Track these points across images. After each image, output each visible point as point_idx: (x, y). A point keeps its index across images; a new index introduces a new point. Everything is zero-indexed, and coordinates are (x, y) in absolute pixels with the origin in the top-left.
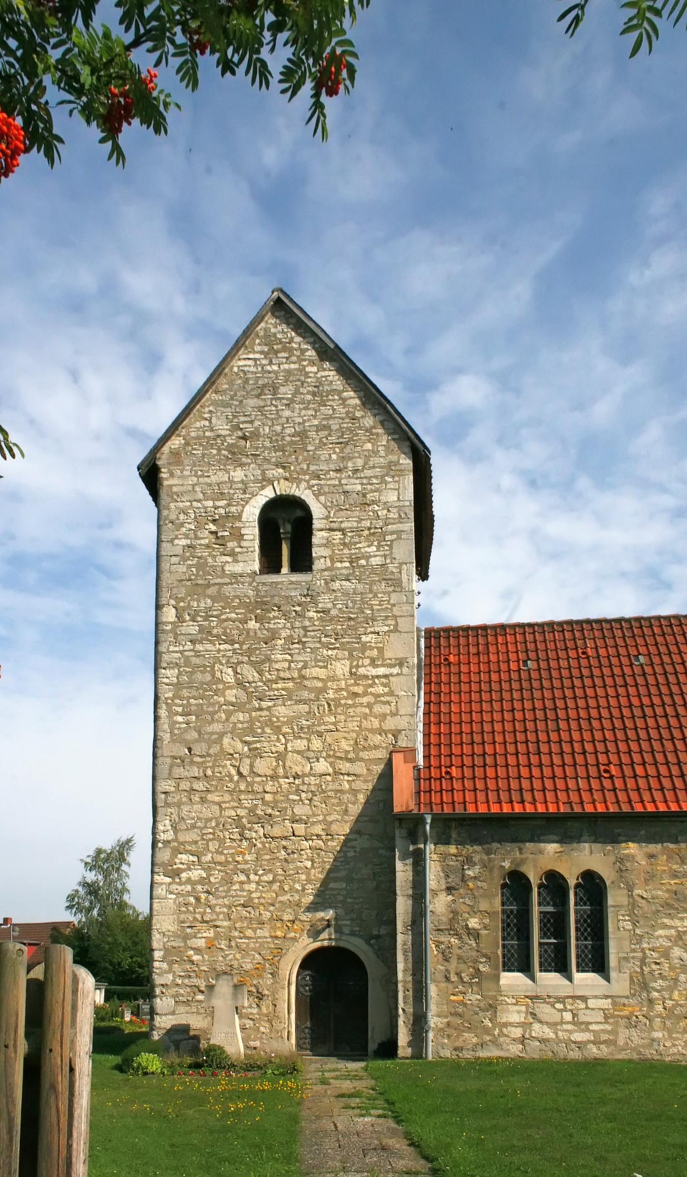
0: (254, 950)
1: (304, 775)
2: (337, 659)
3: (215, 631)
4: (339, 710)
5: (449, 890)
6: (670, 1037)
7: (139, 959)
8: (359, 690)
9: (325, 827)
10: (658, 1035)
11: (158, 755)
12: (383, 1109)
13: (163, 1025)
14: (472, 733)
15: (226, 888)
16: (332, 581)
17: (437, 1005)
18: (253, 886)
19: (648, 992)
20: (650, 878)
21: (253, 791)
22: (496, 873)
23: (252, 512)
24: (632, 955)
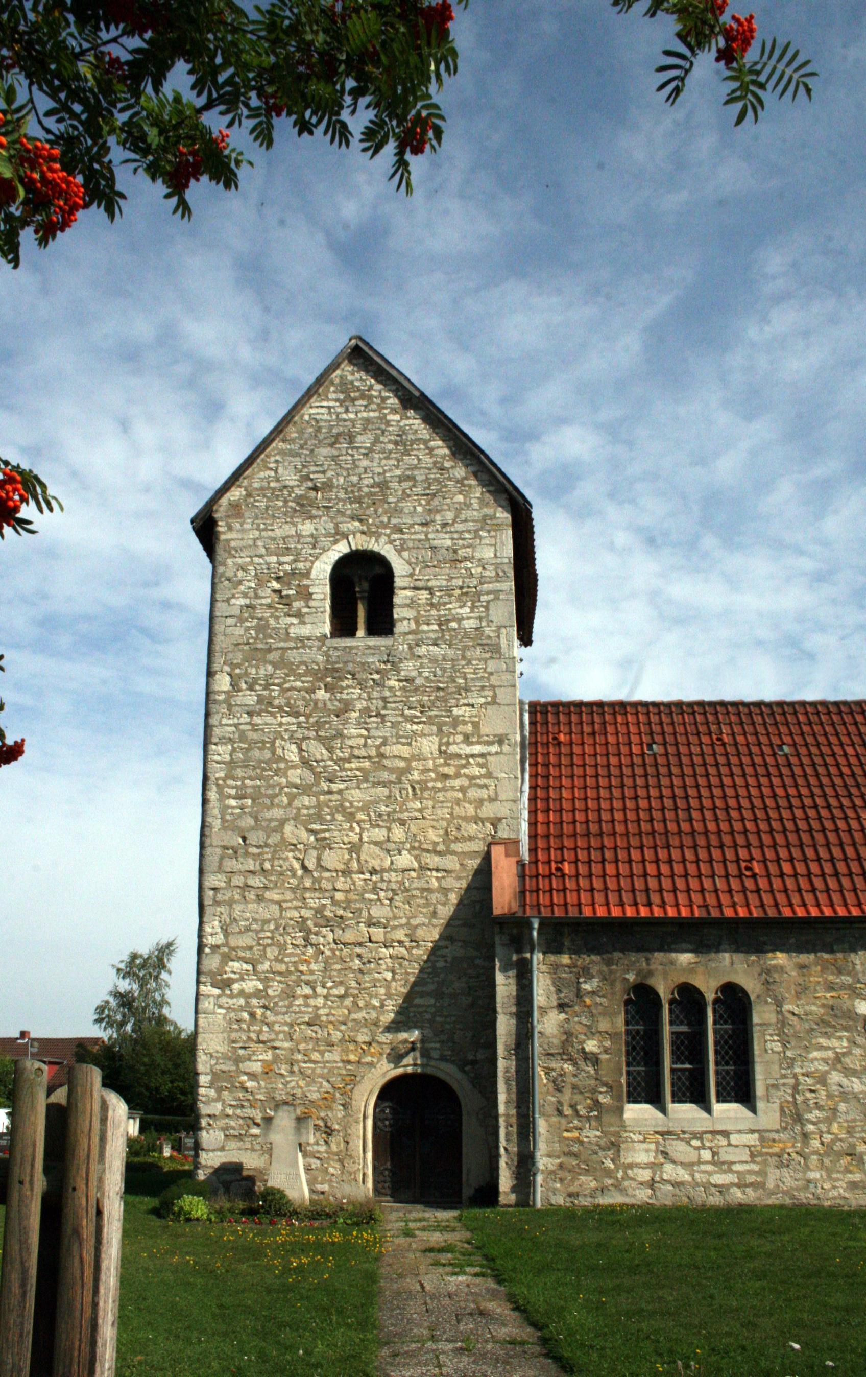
0: (322, 1076)
1: (383, 870)
2: (423, 735)
3: (276, 702)
4: (426, 794)
5: (562, 1007)
6: (829, 1177)
7: (181, 1084)
8: (450, 771)
9: (409, 932)
10: (814, 1175)
11: (207, 844)
12: (482, 1266)
13: (210, 1163)
14: (587, 822)
15: (287, 1002)
16: (418, 645)
17: (548, 1142)
18: (320, 1001)
19: (803, 1125)
20: (802, 991)
21: (320, 888)
22: (619, 987)
23: (323, 568)
24: (782, 1081)
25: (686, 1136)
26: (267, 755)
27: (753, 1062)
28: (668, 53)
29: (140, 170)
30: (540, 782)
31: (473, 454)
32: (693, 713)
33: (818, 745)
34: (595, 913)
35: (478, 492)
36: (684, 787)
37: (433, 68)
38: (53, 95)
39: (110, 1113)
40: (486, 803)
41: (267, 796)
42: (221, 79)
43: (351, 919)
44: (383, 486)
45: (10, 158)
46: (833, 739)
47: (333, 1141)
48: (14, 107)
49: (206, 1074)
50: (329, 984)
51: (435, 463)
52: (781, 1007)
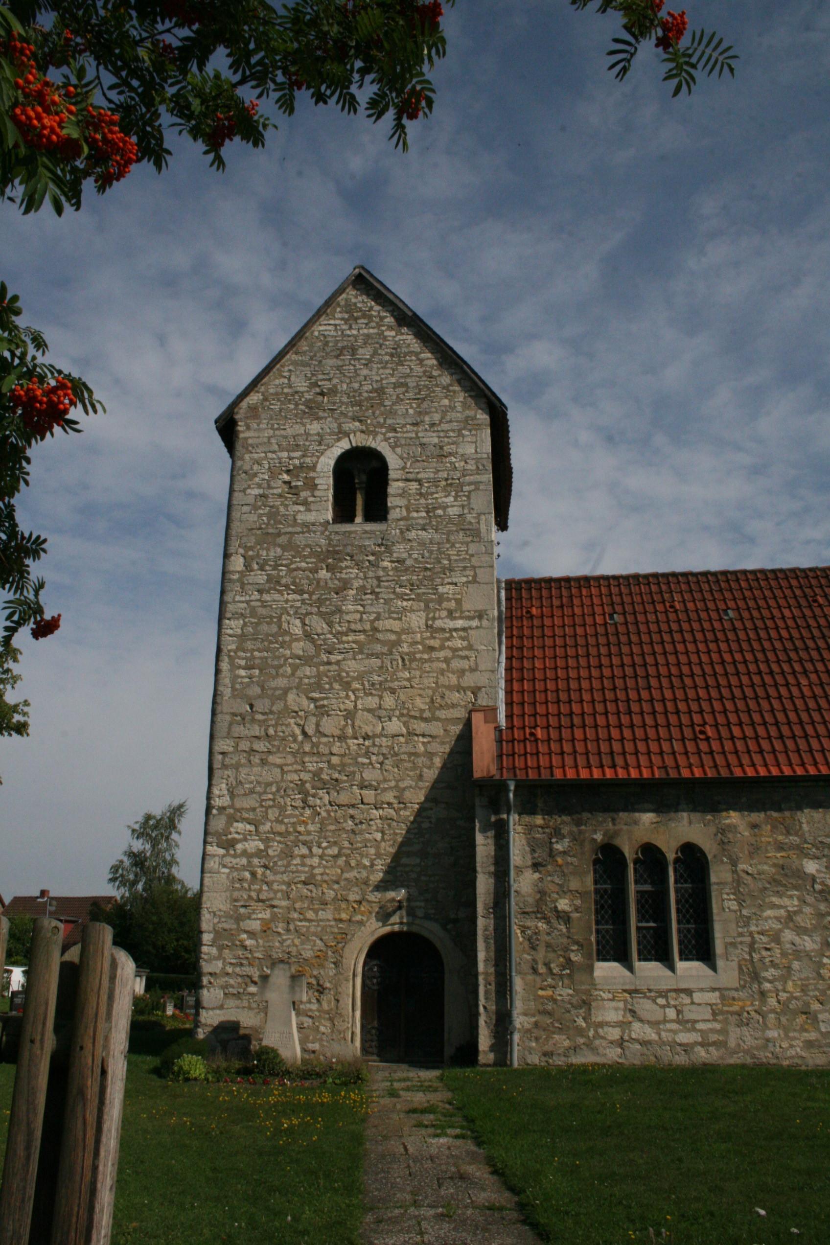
0: (315, 934)
1: (375, 736)
2: (412, 611)
3: (283, 581)
4: (414, 665)
5: (536, 866)
6: (787, 1036)
7: (185, 942)
8: (436, 643)
9: (397, 794)
10: (772, 1034)
11: (218, 711)
12: (462, 1128)
13: (209, 1022)
14: (557, 690)
15: (285, 862)
16: (408, 530)
17: (525, 1000)
18: (316, 861)
19: (760, 983)
20: (755, 850)
21: (318, 753)
22: (587, 847)
23: (327, 462)
24: (739, 939)
25: (652, 994)
26: (274, 629)
27: (712, 921)
28: (616, 41)
29: (185, 132)
30: (515, 654)
31: (457, 364)
32: (649, 584)
33: (758, 608)
34: (565, 775)
35: (461, 396)
36: (643, 654)
37: (426, 52)
38: (116, 73)
39: (119, 971)
40: (467, 673)
41: (273, 667)
42: (253, 61)
43: (345, 782)
44: (380, 391)
45: (79, 122)
46: (772, 603)
47: (325, 999)
48: (84, 82)
49: (209, 932)
50: (324, 844)
51: (425, 372)
52: (736, 866)
